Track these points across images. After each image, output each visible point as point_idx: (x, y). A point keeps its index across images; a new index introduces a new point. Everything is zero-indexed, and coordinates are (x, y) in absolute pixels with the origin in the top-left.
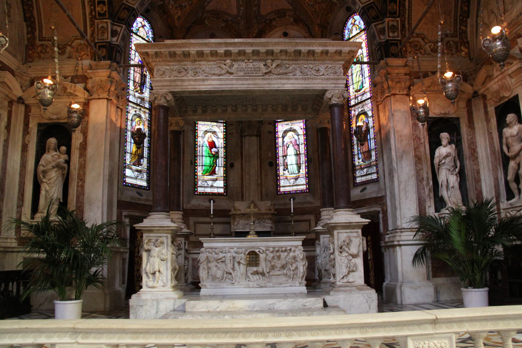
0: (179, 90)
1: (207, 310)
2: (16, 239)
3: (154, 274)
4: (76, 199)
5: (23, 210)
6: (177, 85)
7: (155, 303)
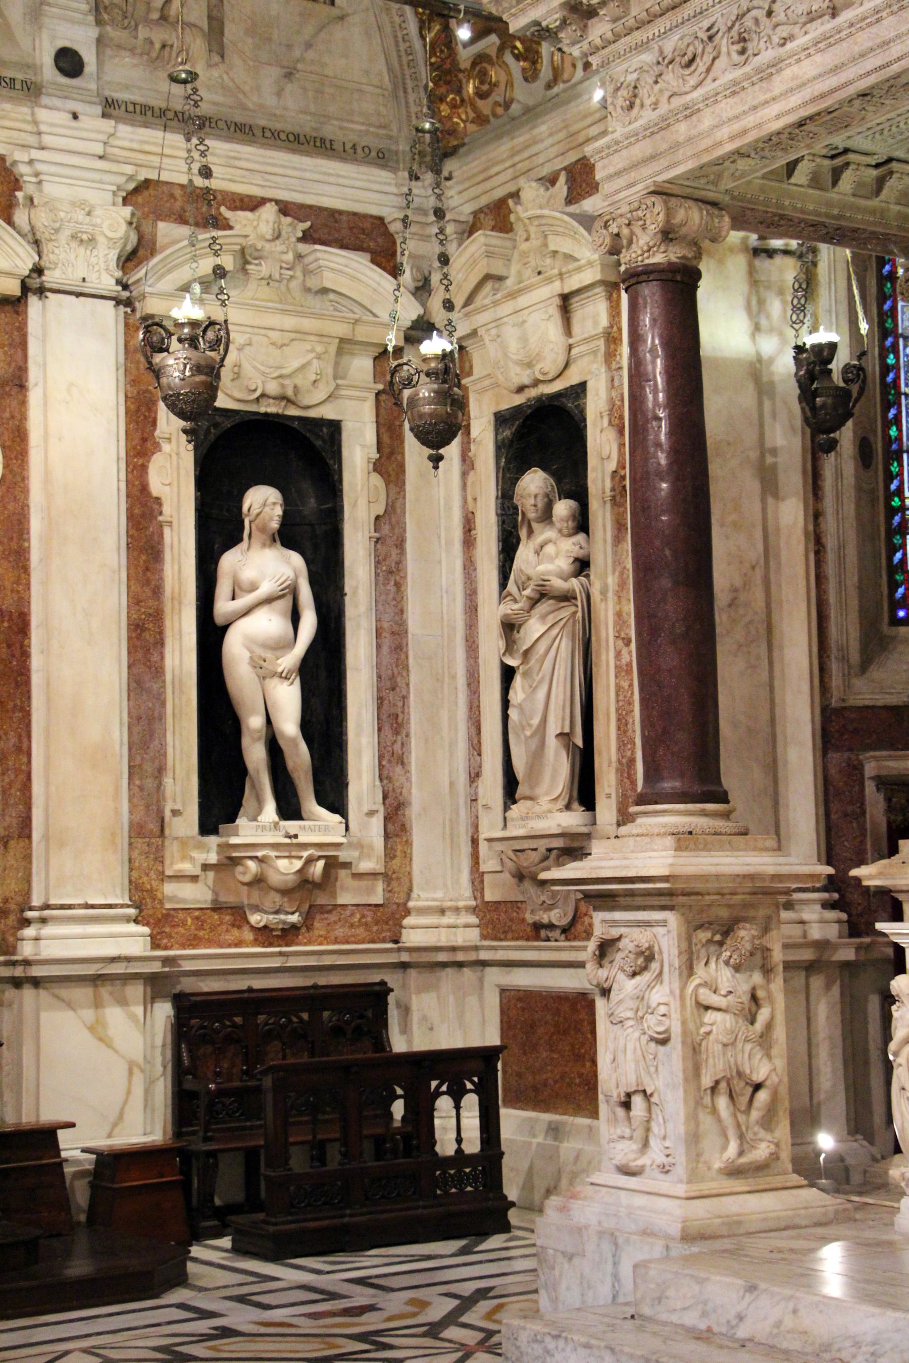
0: (690, 165)
1: (702, 1326)
2: (474, 910)
3: (626, 1105)
4: (619, 729)
5: (481, 791)
6: (676, 146)
7: (607, 1247)
